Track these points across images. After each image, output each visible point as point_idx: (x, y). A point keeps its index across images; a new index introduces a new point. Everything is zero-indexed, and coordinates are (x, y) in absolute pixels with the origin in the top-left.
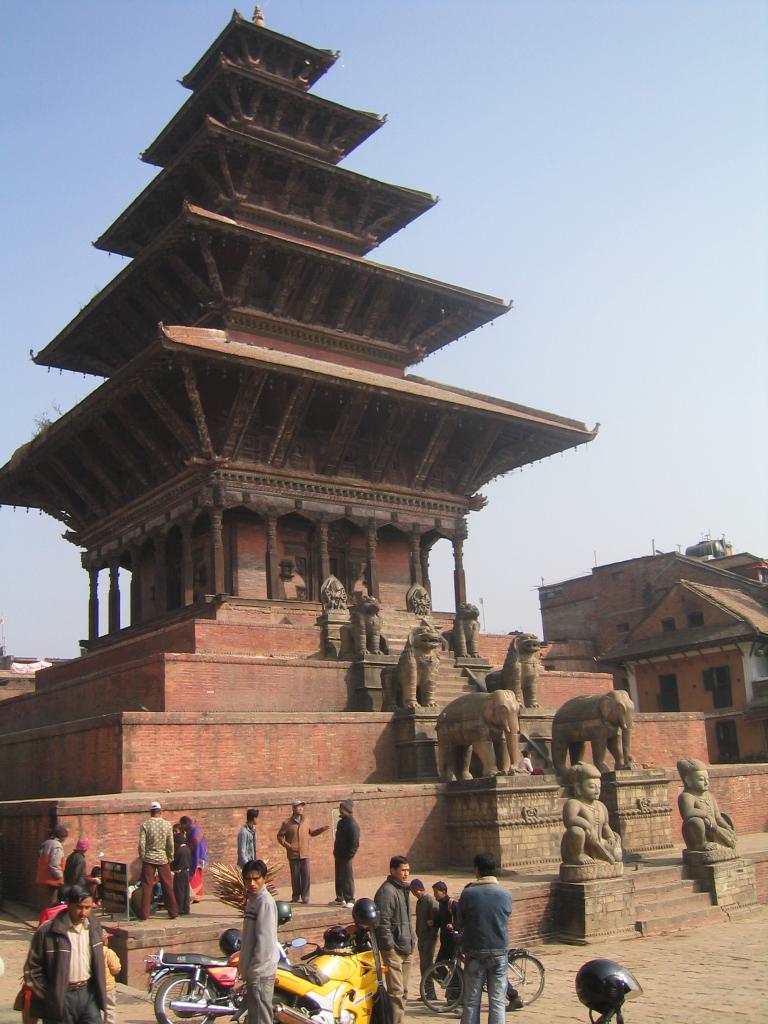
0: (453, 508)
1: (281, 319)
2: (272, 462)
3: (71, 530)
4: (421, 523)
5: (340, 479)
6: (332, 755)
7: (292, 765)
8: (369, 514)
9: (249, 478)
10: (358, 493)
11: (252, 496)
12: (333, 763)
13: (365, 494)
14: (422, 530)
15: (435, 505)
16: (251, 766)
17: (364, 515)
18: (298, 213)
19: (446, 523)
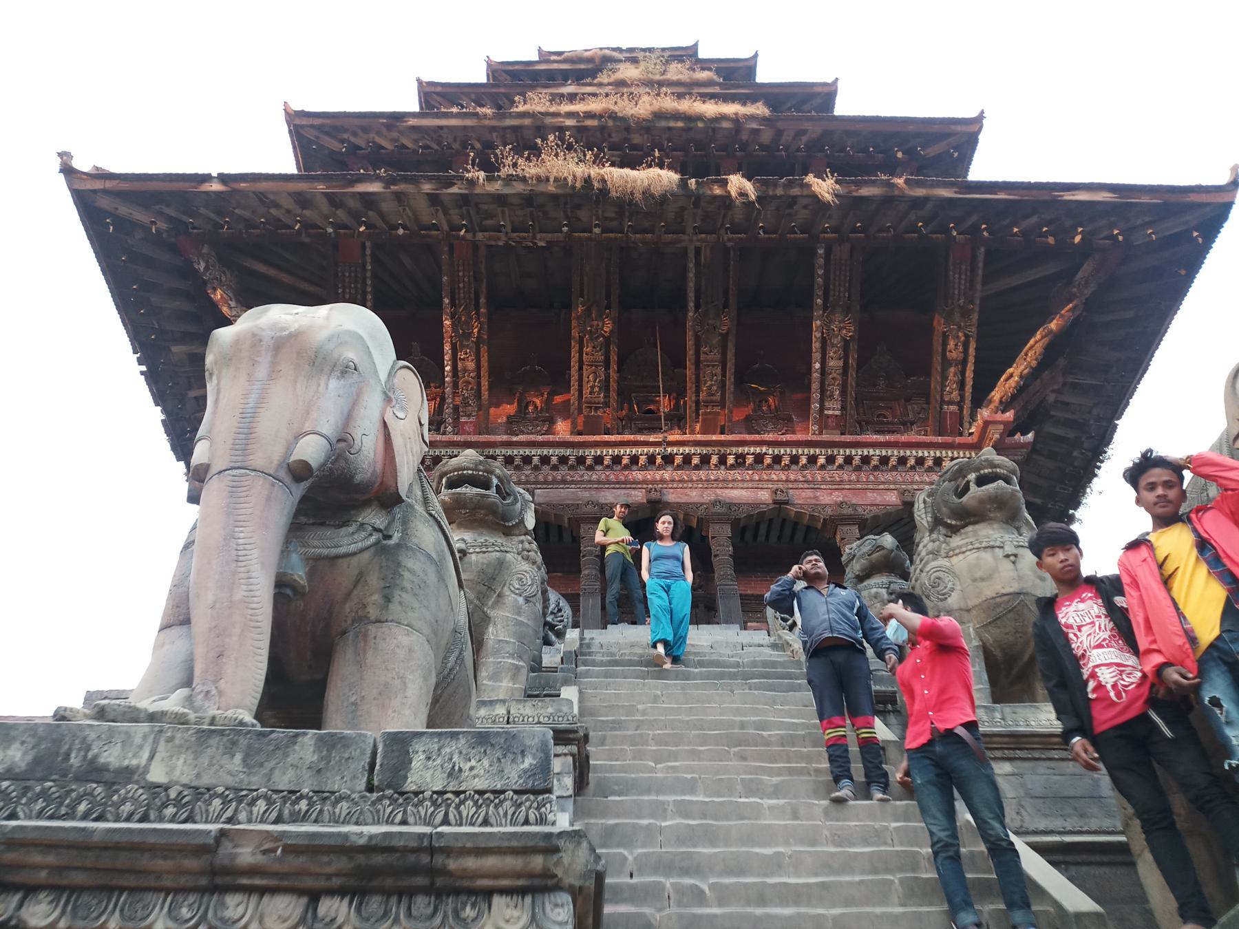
8: (709, 496)
10: (669, 459)
13: (687, 459)
15: (884, 460)
17: (696, 500)
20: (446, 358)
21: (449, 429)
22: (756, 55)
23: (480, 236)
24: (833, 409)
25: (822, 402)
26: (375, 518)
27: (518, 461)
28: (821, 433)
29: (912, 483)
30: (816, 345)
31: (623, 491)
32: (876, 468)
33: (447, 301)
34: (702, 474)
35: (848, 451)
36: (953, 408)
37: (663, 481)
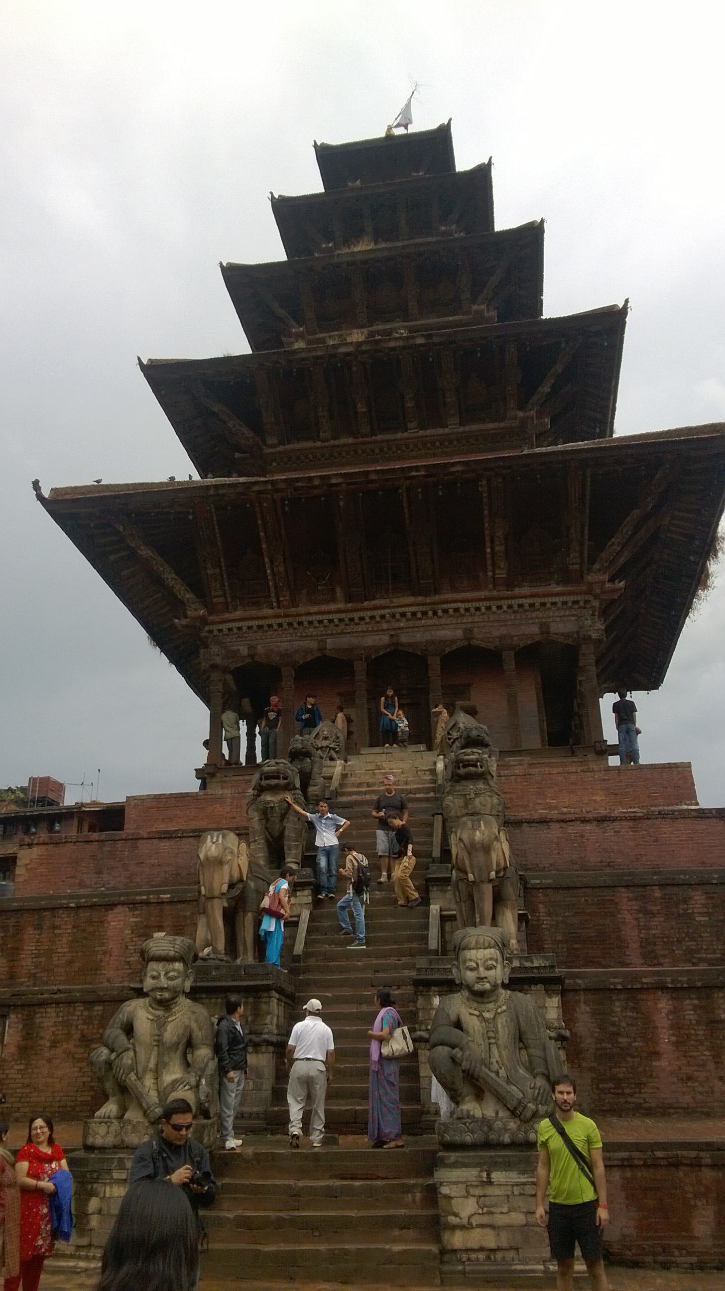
0: (564, 603)
1: (332, 442)
2: (278, 601)
8: (429, 638)
9: (250, 628)
10: (403, 615)
11: (259, 647)
13: (414, 614)
15: (532, 605)
21: (275, 604)
23: (275, 496)
24: (501, 574)
25: (494, 572)
26: (240, 886)
28: (494, 589)
29: (549, 617)
30: (487, 538)
31: (378, 637)
32: (526, 611)
33: (262, 534)
35: (510, 602)
36: (576, 567)
37: (399, 629)
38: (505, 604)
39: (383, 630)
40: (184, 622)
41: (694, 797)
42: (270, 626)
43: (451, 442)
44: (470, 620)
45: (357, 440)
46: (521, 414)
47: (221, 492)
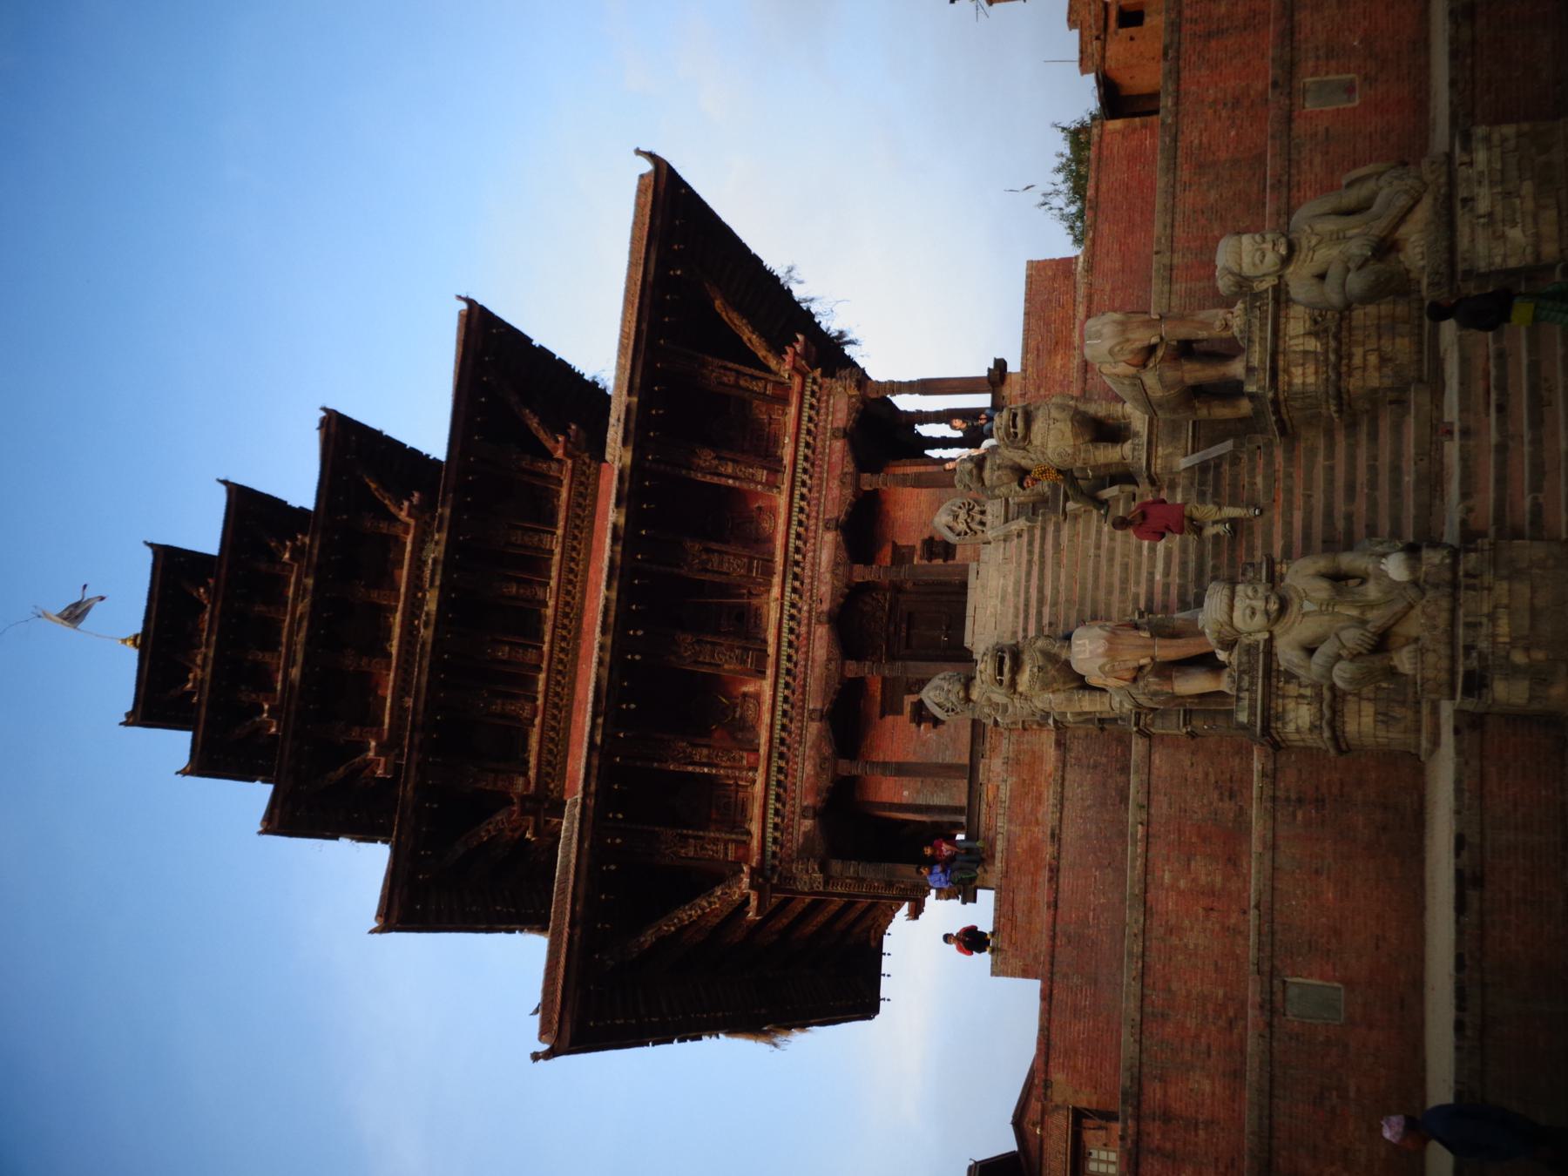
0: (812, 407)
1: (540, 702)
3: (905, 908)
4: (838, 472)
5: (771, 639)
6: (1203, 880)
7: (1217, 969)
8: (828, 577)
9: (777, 812)
12: (1219, 879)
13: (794, 590)
14: (850, 468)
15: (808, 445)
16: (1214, 1053)
18: (389, 639)
19: (839, 415)
20: (698, 770)
22: (225, 482)
24: (763, 475)
27: (786, 721)
30: (716, 480)
34: (807, 581)
36: (769, 387)
37: (810, 611)
38: (800, 476)
39: (809, 633)
40: (754, 902)
41: (1069, 260)
42: (779, 783)
43: (574, 548)
44: (812, 522)
45: (544, 666)
46: (559, 453)
47: (593, 788)
